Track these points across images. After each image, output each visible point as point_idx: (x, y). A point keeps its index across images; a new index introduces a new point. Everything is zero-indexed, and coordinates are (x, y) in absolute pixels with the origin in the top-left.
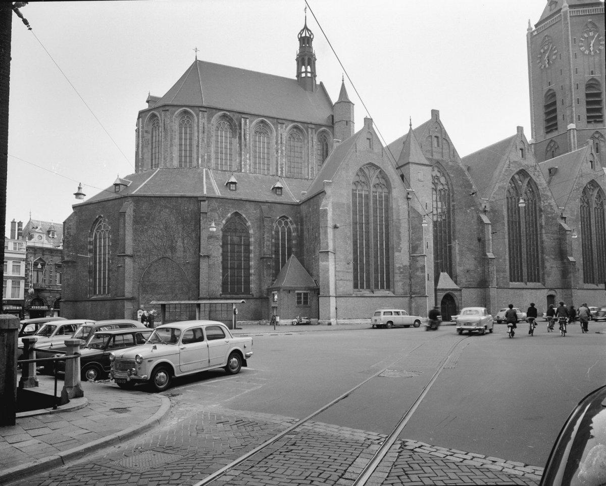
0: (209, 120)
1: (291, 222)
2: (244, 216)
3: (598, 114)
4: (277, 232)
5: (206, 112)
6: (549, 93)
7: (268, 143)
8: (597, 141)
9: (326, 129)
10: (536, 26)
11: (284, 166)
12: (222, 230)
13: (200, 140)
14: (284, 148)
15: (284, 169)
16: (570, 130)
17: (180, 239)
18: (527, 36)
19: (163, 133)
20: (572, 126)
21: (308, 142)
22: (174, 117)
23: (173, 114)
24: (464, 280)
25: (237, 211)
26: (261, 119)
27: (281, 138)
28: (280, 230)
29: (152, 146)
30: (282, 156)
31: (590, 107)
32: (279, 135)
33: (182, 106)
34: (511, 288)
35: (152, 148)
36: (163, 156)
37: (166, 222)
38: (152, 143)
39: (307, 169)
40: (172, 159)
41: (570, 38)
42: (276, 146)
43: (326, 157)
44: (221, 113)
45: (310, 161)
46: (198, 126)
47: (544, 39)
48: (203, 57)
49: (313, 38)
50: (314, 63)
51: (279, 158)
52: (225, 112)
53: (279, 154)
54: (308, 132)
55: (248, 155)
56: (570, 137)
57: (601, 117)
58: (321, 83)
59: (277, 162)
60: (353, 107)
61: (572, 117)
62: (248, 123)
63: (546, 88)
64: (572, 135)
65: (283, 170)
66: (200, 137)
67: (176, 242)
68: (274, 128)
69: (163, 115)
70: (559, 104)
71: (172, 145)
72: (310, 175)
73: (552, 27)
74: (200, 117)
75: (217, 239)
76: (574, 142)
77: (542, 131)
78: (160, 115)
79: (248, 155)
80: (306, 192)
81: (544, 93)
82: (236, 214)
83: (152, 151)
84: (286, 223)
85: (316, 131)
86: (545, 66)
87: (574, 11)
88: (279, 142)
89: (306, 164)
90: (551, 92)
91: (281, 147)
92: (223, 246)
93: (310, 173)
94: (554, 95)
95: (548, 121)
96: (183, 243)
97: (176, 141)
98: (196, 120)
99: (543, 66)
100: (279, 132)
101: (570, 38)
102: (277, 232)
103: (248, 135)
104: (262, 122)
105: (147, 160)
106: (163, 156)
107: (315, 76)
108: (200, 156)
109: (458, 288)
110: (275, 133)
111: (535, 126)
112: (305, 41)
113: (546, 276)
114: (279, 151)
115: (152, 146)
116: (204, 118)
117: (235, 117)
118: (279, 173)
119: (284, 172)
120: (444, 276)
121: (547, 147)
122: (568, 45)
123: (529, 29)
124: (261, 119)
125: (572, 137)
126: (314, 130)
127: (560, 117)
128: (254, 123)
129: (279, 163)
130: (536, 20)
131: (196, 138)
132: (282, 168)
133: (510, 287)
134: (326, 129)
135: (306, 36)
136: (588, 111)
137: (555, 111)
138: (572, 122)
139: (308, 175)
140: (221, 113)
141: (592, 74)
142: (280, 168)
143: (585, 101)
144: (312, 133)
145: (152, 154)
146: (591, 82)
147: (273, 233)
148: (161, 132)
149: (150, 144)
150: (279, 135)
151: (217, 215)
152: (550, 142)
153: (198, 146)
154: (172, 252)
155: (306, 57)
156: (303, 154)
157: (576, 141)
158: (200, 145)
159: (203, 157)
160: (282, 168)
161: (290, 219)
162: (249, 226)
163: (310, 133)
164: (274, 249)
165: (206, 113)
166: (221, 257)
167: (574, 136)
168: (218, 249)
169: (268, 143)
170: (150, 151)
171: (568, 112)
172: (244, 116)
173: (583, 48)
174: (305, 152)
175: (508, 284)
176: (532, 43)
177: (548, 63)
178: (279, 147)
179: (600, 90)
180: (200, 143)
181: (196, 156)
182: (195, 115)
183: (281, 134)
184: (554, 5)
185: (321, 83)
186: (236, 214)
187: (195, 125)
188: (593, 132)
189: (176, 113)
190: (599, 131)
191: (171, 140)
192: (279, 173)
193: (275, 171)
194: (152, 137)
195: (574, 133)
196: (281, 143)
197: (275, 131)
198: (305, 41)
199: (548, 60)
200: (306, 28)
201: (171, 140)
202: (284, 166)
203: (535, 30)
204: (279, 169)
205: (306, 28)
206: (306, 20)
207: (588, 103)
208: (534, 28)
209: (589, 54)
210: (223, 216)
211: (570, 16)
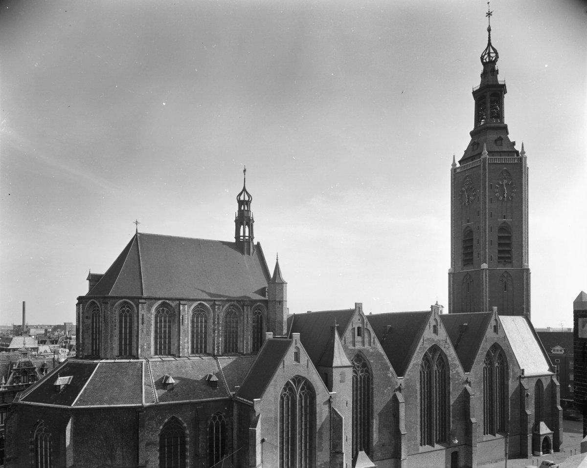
0: (149, 310)
1: (224, 416)
2: (180, 419)
3: (507, 256)
4: (211, 428)
5: (145, 303)
6: (467, 230)
7: (206, 322)
8: (505, 280)
9: (261, 304)
10: (460, 162)
11: (220, 345)
12: (159, 435)
13: (140, 331)
14: (220, 328)
15: (220, 348)
16: (483, 269)
17: (119, 448)
18: (451, 170)
19: (103, 325)
20: (485, 266)
21: (244, 318)
22: (114, 308)
23: (113, 305)
24: (379, 454)
25: (174, 415)
26: (199, 302)
27: (218, 319)
28: (214, 424)
29: (93, 331)
30: (218, 336)
31: (501, 249)
32: (216, 316)
33: (121, 298)
34: (420, 453)
35: (93, 333)
36: (103, 347)
37: (105, 433)
38: (93, 328)
39: (242, 343)
40: (112, 349)
41: (487, 184)
42: (213, 326)
43: (261, 347)
44: (160, 302)
45: (245, 336)
46: (138, 316)
47: (466, 178)
48: (144, 230)
49: (251, 201)
50: (252, 226)
51: (216, 338)
52: (164, 301)
53: (216, 334)
54: (243, 310)
55: (186, 339)
56: (482, 275)
57: (509, 258)
58: (258, 243)
59: (214, 341)
60: (286, 286)
61: (485, 258)
62: (186, 309)
63: (465, 225)
64: (484, 274)
65: (219, 349)
66: (140, 329)
67: (116, 451)
68: (211, 310)
69: (103, 307)
70: (475, 242)
71: (112, 336)
72: (245, 350)
73: (473, 169)
74: (140, 309)
75: (155, 444)
76: (486, 281)
77: (460, 264)
78: (101, 305)
79: (186, 339)
80: (239, 386)
81: (463, 228)
82: (173, 418)
83: (93, 336)
84: (220, 418)
85: (251, 307)
86: (465, 204)
87: (492, 158)
88: (216, 323)
89: (242, 339)
90: (468, 229)
91: (218, 328)
92: (160, 450)
93: (245, 348)
94: (471, 232)
95: (466, 254)
96: (123, 452)
97: (117, 331)
98: (136, 311)
99: (463, 203)
100: (216, 314)
101: (487, 184)
102: (211, 428)
103: (186, 320)
104: (200, 304)
105: (88, 345)
106: (103, 347)
107: (252, 238)
108: (140, 347)
109: (374, 444)
110: (212, 314)
111: (454, 257)
112: (244, 204)
113: (451, 436)
114: (216, 332)
115: (93, 331)
116: (144, 309)
117: (173, 304)
118: (216, 351)
119: (220, 350)
120: (362, 454)
121: (463, 279)
122: (485, 190)
123: (454, 165)
124: (199, 302)
125: (484, 276)
126: (249, 307)
127: (475, 255)
128: (192, 307)
129: (216, 342)
130: (460, 156)
131: (136, 328)
132: (218, 347)
133: (420, 452)
134: (261, 304)
135: (244, 200)
136: (500, 252)
137: (471, 247)
138: (485, 262)
139: (243, 350)
140: (160, 302)
141: (504, 219)
142: (217, 347)
143: (497, 257)
144: (247, 310)
145: (93, 339)
146: (503, 225)
147: (208, 429)
148: (101, 322)
149: (91, 329)
150: (216, 316)
151: (154, 422)
152: (466, 275)
153: (137, 336)
154: (111, 460)
155: (244, 219)
156: (239, 329)
157: (488, 280)
158: (140, 336)
159: (142, 347)
160: (218, 347)
161: (224, 414)
162: (185, 427)
163: (245, 310)
164: (208, 444)
165: (146, 304)
166: (158, 461)
167: (486, 275)
168: (156, 454)
169: (206, 322)
170: (91, 336)
171: (482, 253)
172: (181, 302)
173: (498, 194)
174: (240, 327)
175: (418, 449)
176: (454, 179)
177: (468, 202)
178: (216, 327)
179: (510, 234)
180: (140, 334)
181: (136, 345)
182: (134, 306)
183: (218, 315)
184: (476, 146)
185: (258, 243)
186: (173, 418)
187: (135, 316)
188: (504, 270)
189: (117, 304)
190: (508, 271)
191: (111, 331)
192: (216, 351)
193: (212, 350)
194: (93, 323)
195: (486, 273)
196: (218, 323)
197: (212, 312)
198: (244, 204)
199: (468, 198)
200: (244, 190)
201: (111, 331)
202: (220, 345)
203: (458, 168)
204: (216, 348)
205: (244, 190)
206: (245, 182)
207: (500, 245)
208: (458, 165)
209: (503, 200)
210: (160, 422)
211: (489, 163)
